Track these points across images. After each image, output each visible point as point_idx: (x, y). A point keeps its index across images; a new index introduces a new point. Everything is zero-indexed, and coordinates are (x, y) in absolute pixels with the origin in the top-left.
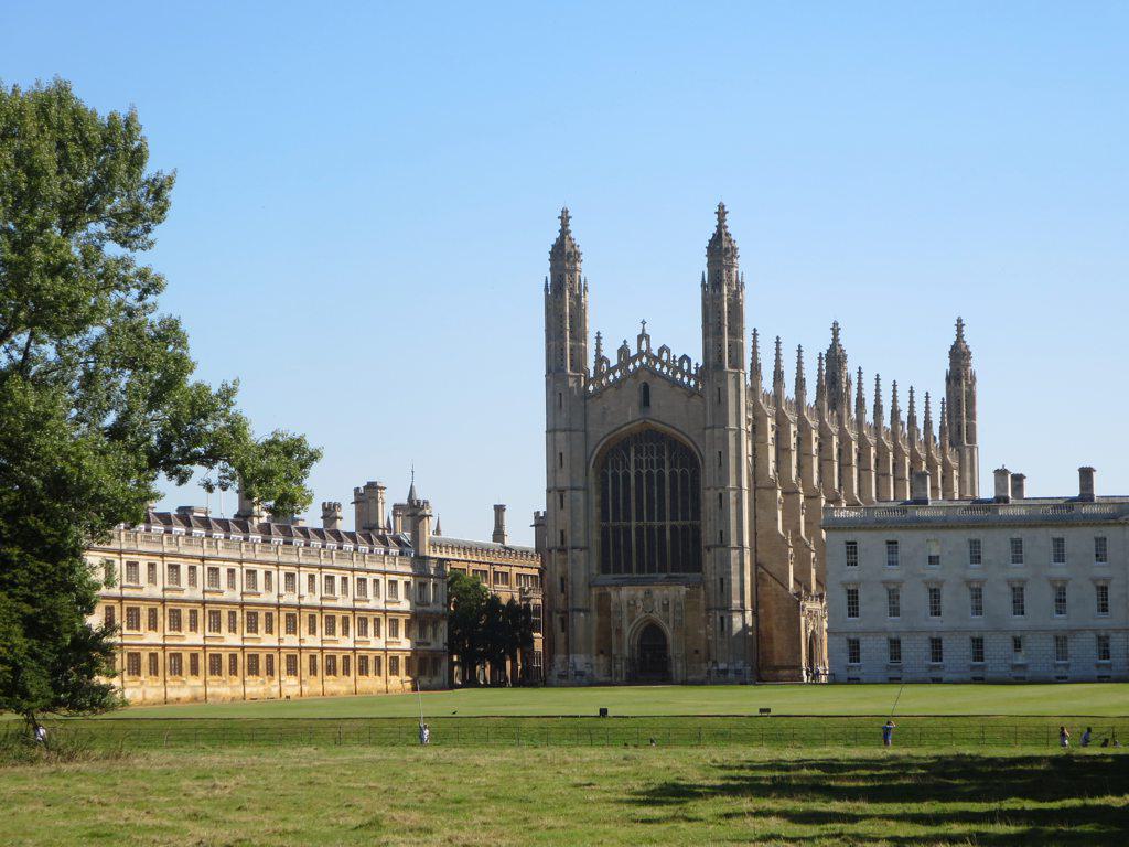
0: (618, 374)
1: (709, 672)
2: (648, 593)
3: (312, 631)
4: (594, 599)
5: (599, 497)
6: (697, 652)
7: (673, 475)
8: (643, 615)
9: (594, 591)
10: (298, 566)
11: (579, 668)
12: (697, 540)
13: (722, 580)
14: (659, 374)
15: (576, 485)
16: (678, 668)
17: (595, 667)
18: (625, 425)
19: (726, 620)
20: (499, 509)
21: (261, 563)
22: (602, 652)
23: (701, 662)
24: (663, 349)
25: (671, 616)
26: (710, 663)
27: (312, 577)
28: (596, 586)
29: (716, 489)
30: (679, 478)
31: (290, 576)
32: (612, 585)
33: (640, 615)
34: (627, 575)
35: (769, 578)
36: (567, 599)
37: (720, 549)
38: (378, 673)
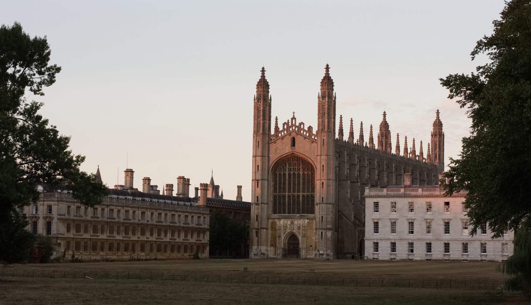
0: (283, 133)
1: (316, 255)
2: (292, 223)
3: (152, 235)
4: (270, 224)
5: (273, 183)
6: (311, 246)
7: (304, 174)
8: (290, 231)
9: (270, 221)
10: (147, 209)
11: (262, 252)
12: (313, 201)
13: (322, 217)
15: (264, 178)
16: (303, 253)
17: (269, 251)
18: (285, 154)
19: (323, 233)
20: (240, 188)
21: (132, 207)
22: (272, 245)
23: (312, 250)
24: (302, 123)
25: (301, 231)
26: (316, 251)
27: (152, 214)
28: (270, 218)
29: (322, 180)
30: (306, 175)
31: (143, 213)
32: (277, 219)
33: (288, 231)
34: (284, 215)
35: (344, 217)
36: (258, 224)
37: (322, 205)
38: (179, 251)
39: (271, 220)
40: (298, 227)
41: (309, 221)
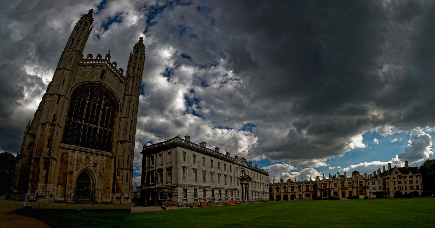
7: (104, 108)
8: (84, 167)
9: (61, 151)
14: (109, 69)
19: (129, 175)
33: (82, 167)
39: (63, 149)
40: (94, 163)
41: (107, 158)
